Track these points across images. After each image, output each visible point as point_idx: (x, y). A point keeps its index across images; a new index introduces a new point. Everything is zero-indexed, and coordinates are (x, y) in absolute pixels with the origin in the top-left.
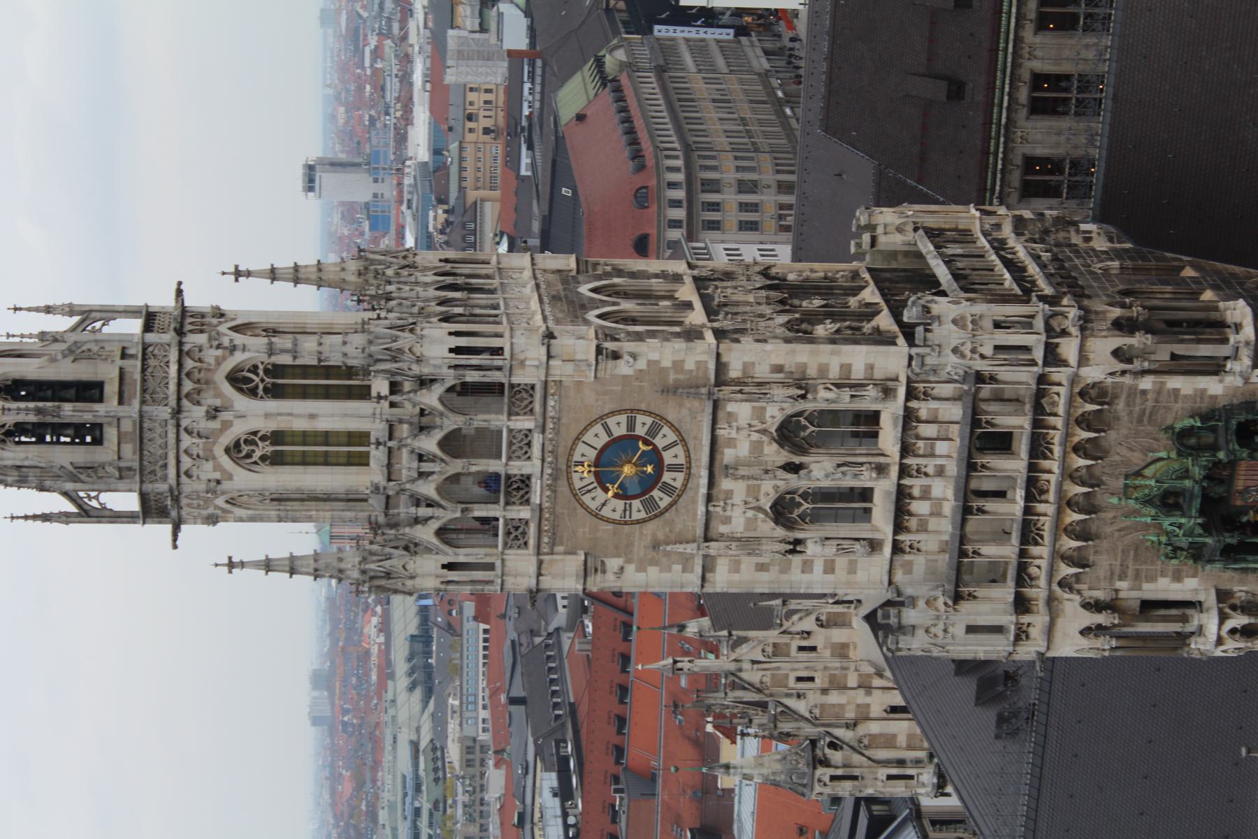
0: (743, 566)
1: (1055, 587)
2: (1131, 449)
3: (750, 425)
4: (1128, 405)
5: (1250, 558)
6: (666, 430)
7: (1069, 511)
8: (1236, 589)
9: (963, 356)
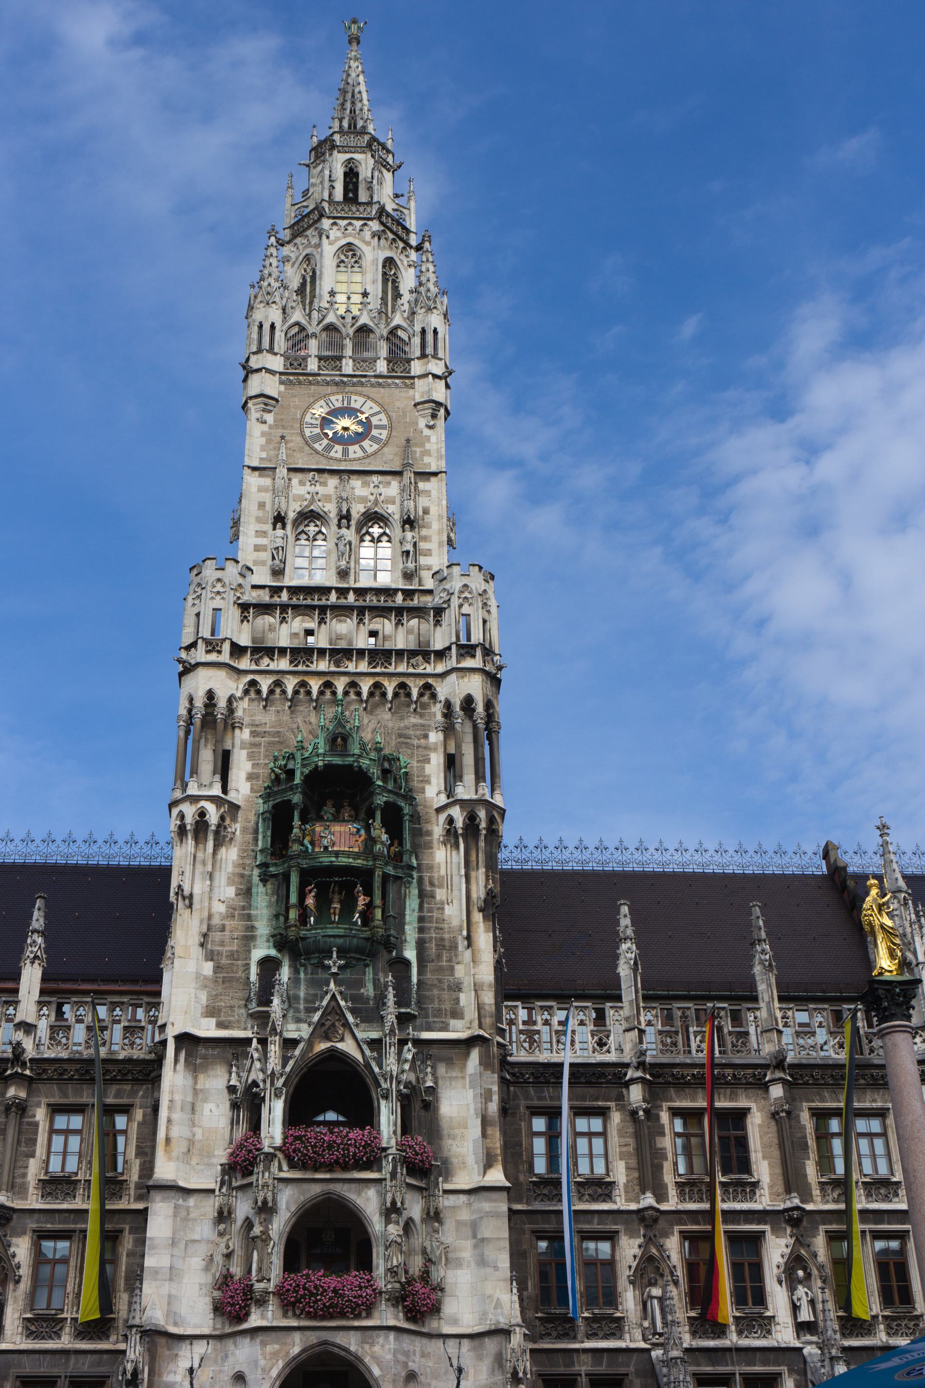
0: (263, 494)
1: (250, 677)
2: (374, 730)
3: (380, 495)
4: (414, 725)
5: (269, 833)
6: (375, 447)
7: (321, 682)
8: (238, 826)
9: (461, 592)
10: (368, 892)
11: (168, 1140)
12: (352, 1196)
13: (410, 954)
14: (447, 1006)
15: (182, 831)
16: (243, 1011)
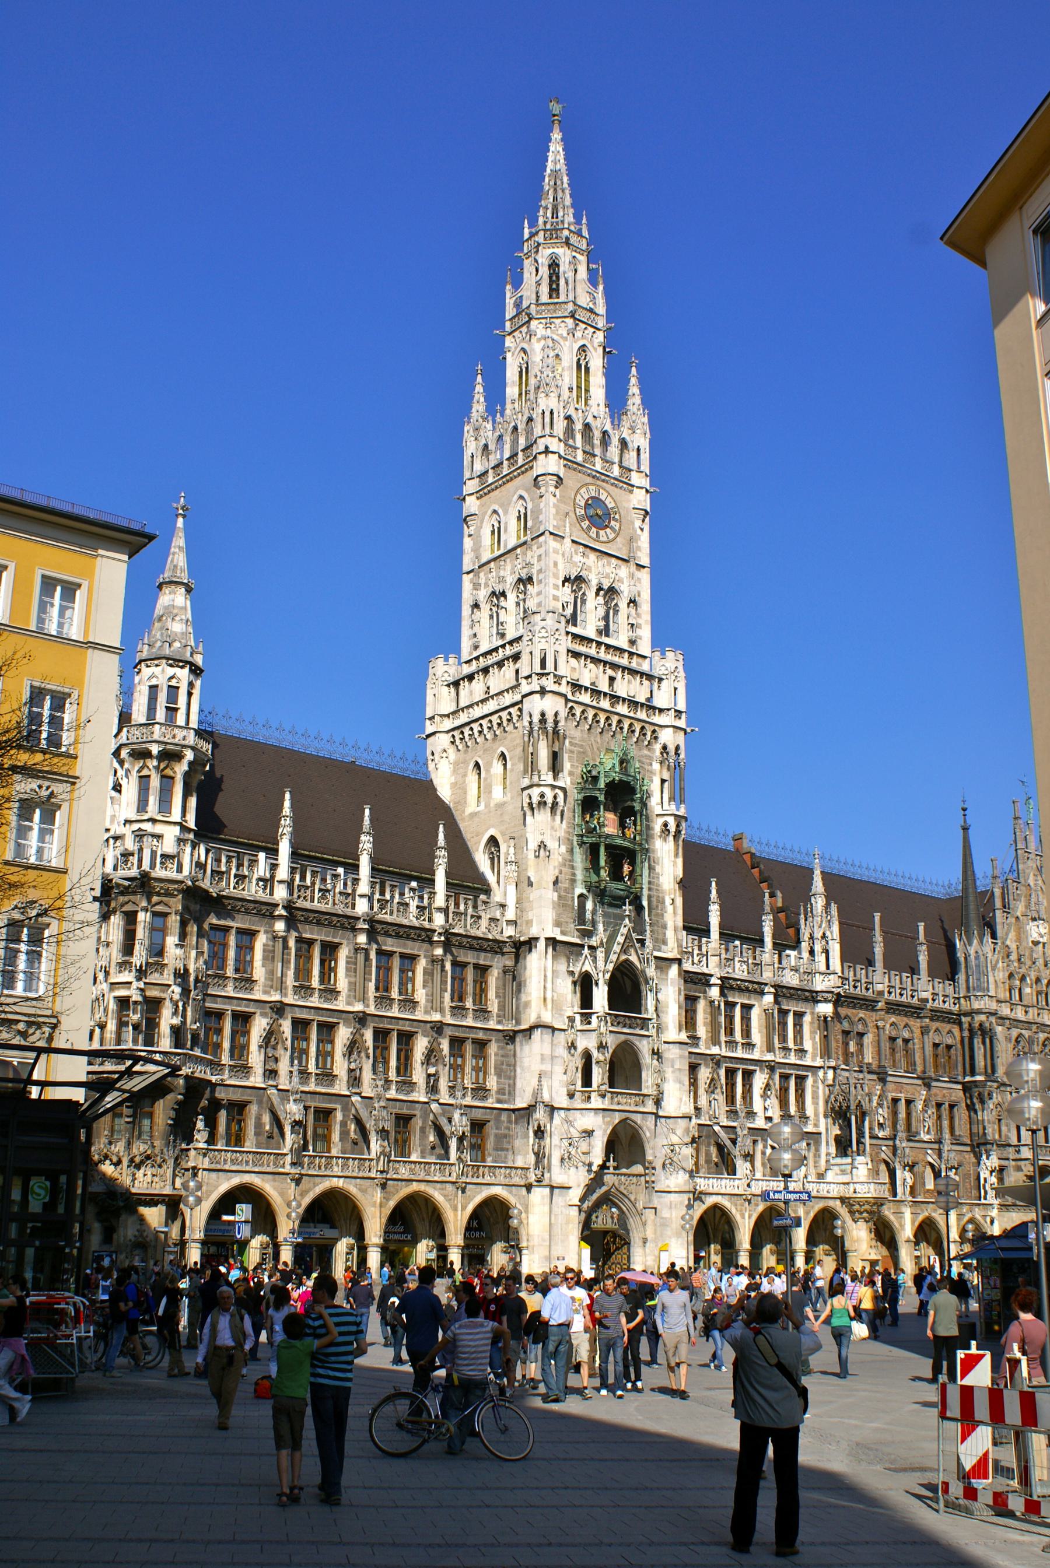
1: (570, 704)
10: (632, 863)
11: (545, 999)
12: (637, 1043)
13: (645, 903)
14: (660, 937)
15: (542, 803)
16: (572, 926)
